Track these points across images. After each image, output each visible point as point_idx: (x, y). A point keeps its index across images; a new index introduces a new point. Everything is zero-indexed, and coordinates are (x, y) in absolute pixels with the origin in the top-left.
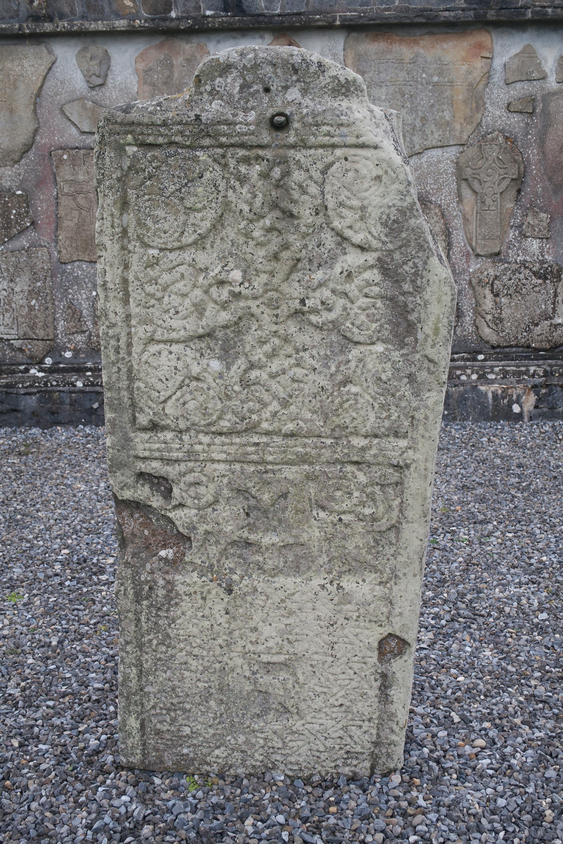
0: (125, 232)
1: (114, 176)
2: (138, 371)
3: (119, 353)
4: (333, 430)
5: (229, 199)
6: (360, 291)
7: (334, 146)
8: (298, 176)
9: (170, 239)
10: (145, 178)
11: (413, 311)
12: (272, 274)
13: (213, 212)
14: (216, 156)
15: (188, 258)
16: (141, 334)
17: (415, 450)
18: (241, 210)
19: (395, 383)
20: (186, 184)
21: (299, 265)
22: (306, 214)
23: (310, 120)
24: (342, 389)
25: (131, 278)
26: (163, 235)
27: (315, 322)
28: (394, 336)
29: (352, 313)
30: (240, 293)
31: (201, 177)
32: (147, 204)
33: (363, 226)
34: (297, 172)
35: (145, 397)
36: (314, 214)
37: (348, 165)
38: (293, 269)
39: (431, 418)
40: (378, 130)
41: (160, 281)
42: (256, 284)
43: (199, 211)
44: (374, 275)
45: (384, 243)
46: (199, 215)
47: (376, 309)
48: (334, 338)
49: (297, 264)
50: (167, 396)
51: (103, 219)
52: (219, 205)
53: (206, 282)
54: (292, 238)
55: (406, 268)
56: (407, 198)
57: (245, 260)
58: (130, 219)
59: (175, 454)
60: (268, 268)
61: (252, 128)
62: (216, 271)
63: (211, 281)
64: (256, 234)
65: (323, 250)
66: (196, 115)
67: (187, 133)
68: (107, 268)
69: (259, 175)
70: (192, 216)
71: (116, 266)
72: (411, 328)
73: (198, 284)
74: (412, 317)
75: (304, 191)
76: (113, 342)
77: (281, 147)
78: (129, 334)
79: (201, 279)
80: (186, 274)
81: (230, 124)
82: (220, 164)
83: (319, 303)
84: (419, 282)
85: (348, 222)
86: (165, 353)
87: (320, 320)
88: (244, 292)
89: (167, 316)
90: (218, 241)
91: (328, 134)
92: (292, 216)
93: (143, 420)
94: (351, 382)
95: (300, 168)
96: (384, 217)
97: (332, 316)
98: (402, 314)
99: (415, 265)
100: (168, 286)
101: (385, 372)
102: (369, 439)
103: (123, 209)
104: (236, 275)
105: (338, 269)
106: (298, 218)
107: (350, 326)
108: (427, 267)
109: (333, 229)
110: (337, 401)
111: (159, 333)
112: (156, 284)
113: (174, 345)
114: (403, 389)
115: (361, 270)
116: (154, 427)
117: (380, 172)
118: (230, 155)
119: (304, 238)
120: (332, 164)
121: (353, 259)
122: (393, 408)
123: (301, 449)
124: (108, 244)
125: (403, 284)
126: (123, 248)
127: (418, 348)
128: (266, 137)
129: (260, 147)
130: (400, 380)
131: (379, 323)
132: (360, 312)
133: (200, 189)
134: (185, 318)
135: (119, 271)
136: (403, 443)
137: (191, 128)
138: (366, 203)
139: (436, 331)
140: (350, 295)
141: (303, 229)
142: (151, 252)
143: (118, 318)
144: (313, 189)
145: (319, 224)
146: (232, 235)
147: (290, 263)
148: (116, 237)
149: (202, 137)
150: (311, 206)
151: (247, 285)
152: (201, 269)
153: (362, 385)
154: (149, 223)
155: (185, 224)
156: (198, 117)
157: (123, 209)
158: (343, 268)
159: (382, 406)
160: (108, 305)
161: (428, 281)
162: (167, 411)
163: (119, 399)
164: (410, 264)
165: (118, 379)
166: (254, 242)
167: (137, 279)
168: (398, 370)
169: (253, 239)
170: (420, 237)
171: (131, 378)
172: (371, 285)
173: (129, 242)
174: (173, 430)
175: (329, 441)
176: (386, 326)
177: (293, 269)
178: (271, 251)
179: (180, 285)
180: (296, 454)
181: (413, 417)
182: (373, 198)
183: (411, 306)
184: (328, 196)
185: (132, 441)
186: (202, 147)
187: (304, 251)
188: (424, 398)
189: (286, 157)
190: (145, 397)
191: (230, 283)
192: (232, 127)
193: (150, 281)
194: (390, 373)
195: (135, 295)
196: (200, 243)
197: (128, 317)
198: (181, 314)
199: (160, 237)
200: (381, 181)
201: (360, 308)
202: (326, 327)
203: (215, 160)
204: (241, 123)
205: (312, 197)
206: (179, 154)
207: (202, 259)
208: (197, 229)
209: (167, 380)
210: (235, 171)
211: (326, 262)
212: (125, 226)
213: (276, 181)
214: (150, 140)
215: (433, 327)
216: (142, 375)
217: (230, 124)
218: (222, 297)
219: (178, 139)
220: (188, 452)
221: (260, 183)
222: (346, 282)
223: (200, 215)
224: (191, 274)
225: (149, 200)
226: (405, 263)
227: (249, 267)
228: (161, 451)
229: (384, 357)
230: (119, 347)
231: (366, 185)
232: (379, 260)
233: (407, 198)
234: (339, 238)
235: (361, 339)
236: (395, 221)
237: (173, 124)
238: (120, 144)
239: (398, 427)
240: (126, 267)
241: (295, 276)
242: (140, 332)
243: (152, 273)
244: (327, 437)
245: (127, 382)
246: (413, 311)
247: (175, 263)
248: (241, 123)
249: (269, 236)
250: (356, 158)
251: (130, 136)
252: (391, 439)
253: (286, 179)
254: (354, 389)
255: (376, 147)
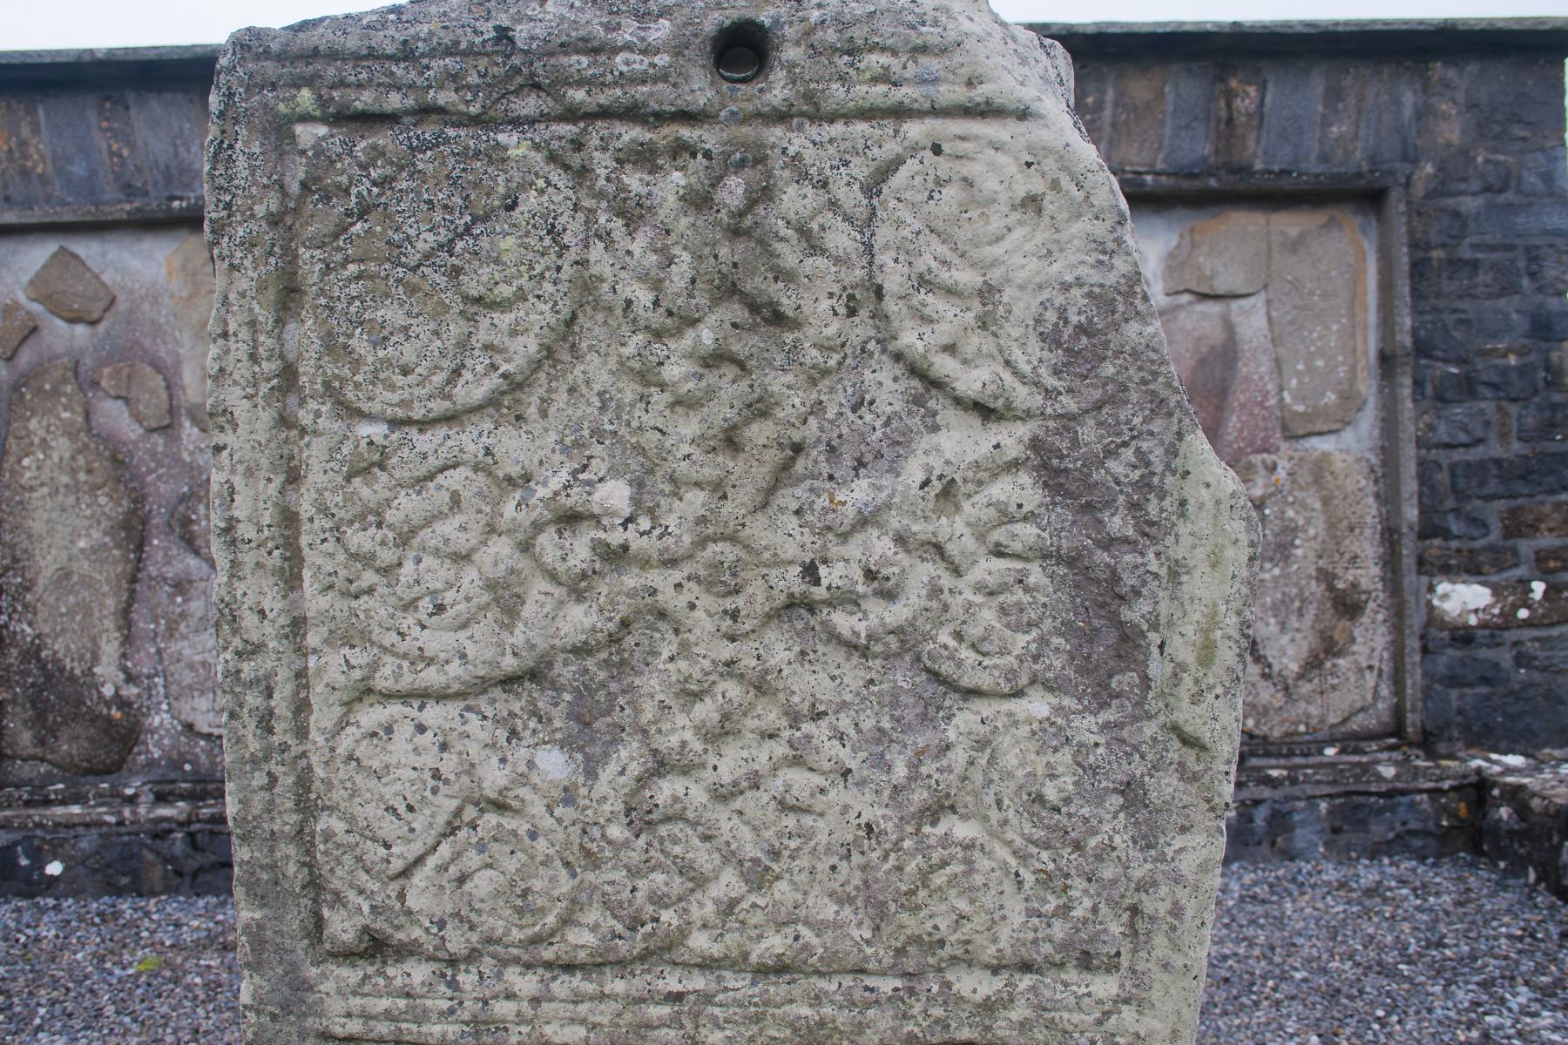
0: (289, 374)
1: (260, 210)
2: (328, 783)
3: (270, 730)
4: (901, 952)
5: (595, 270)
6: (981, 538)
7: (900, 113)
8: (794, 200)
9: (417, 391)
10: (349, 214)
11: (1138, 594)
12: (719, 489)
13: (546, 308)
14: (555, 145)
15: (471, 447)
16: (334, 674)
17: (1141, 1005)
18: (629, 303)
19: (1085, 811)
20: (468, 229)
21: (800, 466)
22: (820, 312)
23: (831, 36)
24: (927, 829)
25: (306, 508)
26: (399, 380)
27: (845, 631)
28: (1080, 671)
29: (956, 603)
30: (625, 548)
31: (510, 208)
32: (355, 288)
33: (989, 345)
34: (792, 190)
35: (348, 860)
36: (842, 311)
37: (944, 166)
38: (783, 474)
39: (1189, 913)
40: (1026, 70)
41: (390, 516)
42: (671, 521)
43: (503, 305)
44: (1021, 489)
45: (1050, 394)
46: (505, 320)
47: (1027, 590)
48: (902, 678)
49: (793, 459)
50: (411, 857)
51: (225, 335)
52: (563, 287)
53: (525, 518)
54: (777, 383)
55: (1115, 466)
56: (1117, 261)
57: (640, 449)
58: (303, 335)
59: (437, 1029)
60: (709, 473)
61: (662, 60)
62: (555, 484)
63: (539, 512)
64: (673, 371)
65: (868, 417)
66: (498, 28)
67: (473, 79)
68: (238, 481)
69: (682, 198)
70: (484, 323)
71: (263, 474)
72: (1129, 644)
73: (502, 524)
74: (1135, 613)
75: (812, 244)
76: (253, 699)
77: (746, 119)
78: (301, 674)
79: (509, 509)
80: (466, 494)
81: (596, 51)
82: (566, 168)
83: (857, 574)
84: (1153, 509)
85: (943, 332)
86: (404, 730)
87: (862, 627)
88: (637, 544)
89: (411, 621)
90: (561, 397)
91: (884, 77)
92: (777, 318)
93: (342, 927)
94: (953, 809)
95: (803, 176)
96: (1051, 316)
97: (897, 614)
98: (1102, 606)
99: (1143, 459)
100: (413, 532)
101: (1053, 777)
102: (1005, 975)
103: (285, 308)
104: (615, 495)
105: (913, 472)
106: (795, 324)
107: (952, 643)
108: (1177, 463)
109: (898, 357)
110: (911, 867)
111: (387, 671)
112: (379, 525)
113: (431, 704)
114: (1106, 827)
115: (984, 475)
116: (375, 948)
117: (1038, 186)
118: (595, 141)
119: (813, 382)
120: (896, 163)
121: (959, 442)
122: (1078, 884)
123: (805, 1011)
124: (241, 409)
125: (1105, 516)
126: (284, 421)
127: (1153, 705)
128: (700, 89)
129: (686, 116)
130: (1099, 801)
131: (1035, 633)
132: (979, 599)
133: (509, 242)
134: (464, 626)
135: (273, 489)
136: (1105, 986)
137: (483, 63)
138: (995, 275)
139: (1207, 653)
140: (950, 548)
141: (812, 355)
142: (365, 430)
143: (268, 629)
144: (841, 239)
145: (857, 341)
146: (602, 379)
147: (773, 456)
148: (264, 388)
149: (516, 92)
150: (836, 289)
151: (645, 523)
152: (509, 479)
153: (986, 818)
154: (360, 343)
155: (464, 345)
156: (503, 34)
157: (285, 308)
158: (929, 469)
159: (1046, 880)
160: (240, 588)
161: (1183, 503)
162: (412, 902)
163: (273, 866)
164: (1128, 454)
165: (270, 808)
166: (667, 397)
167: (325, 511)
168: (1094, 770)
169: (662, 386)
170: (1155, 374)
171: (307, 805)
172: (1012, 520)
173: (302, 402)
174: (431, 958)
175: (887, 985)
176: (1057, 641)
177: (783, 474)
178: (718, 422)
179: (447, 528)
180: (791, 1025)
181: (1135, 910)
182: (1017, 260)
183: (1130, 580)
184: (885, 258)
185: (311, 989)
186: (516, 122)
187: (812, 421)
188: (1169, 852)
189: (761, 145)
190: (348, 860)
191: (596, 519)
192: (602, 58)
193: (362, 517)
194: (1069, 780)
195: (318, 558)
196: (506, 402)
197: (297, 625)
198: (451, 612)
199: (392, 387)
200: (1039, 211)
201: (979, 588)
202: (878, 648)
203: (552, 158)
204: (628, 47)
205: (837, 261)
206: (447, 141)
207: (514, 449)
208: (498, 359)
209: (410, 808)
210: (611, 188)
211: (879, 455)
212: (291, 357)
213: (732, 215)
214: (364, 100)
215: (1198, 639)
216: (338, 795)
217: (596, 51)
218: (571, 562)
219: (446, 97)
220: (475, 1020)
221: (684, 222)
222: (939, 512)
223: (509, 318)
224: (480, 494)
225: (359, 277)
226: (1110, 453)
227: (651, 472)
228: (395, 1020)
229: (1051, 735)
230: (271, 713)
231: (996, 224)
232: (1035, 444)
233: (1117, 261)
234: (916, 383)
235: (985, 681)
236: (1081, 329)
237: (432, 54)
238: (276, 115)
239: (1093, 939)
240: (294, 477)
241: (788, 498)
242: (333, 668)
243: (366, 492)
244: (883, 974)
245: (295, 818)
246: (1138, 594)
247: (433, 462)
248: (628, 47)
249: (711, 378)
250: (966, 145)
251: (306, 93)
252: (1071, 975)
253: (760, 210)
254: (963, 830)
255: (1023, 115)
